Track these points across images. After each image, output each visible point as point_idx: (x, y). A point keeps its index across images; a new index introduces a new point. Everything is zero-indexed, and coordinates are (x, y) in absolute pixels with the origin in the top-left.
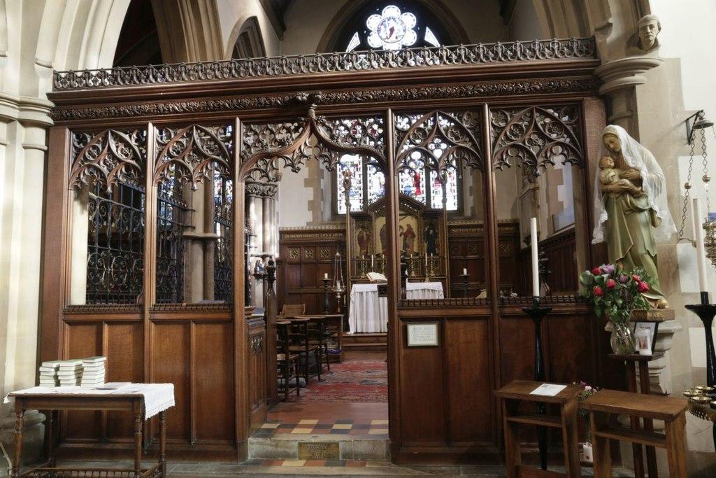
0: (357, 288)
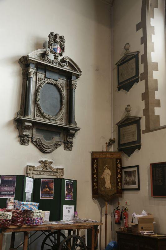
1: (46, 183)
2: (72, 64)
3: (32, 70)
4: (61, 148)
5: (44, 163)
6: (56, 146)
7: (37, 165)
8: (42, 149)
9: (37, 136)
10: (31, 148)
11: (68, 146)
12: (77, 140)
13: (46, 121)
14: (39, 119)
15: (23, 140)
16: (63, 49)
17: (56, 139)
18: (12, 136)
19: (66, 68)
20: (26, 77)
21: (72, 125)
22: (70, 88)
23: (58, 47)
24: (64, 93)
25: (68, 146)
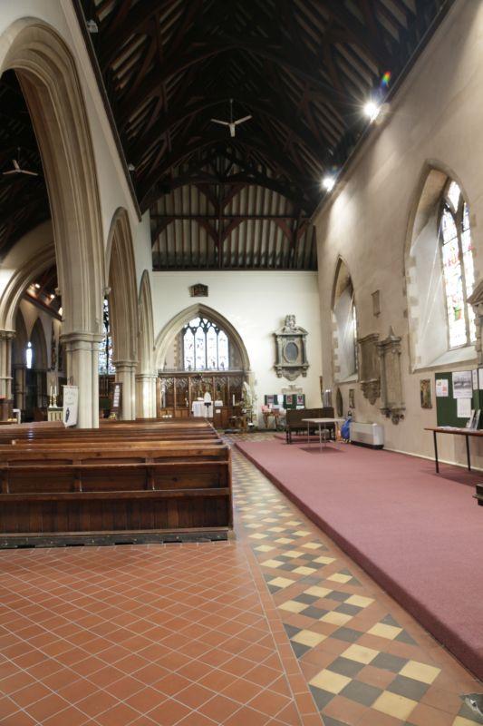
0: (194, 403)
1: (289, 397)
2: (301, 329)
3: (279, 340)
4: (300, 377)
5: (291, 386)
6: (297, 376)
7: (287, 387)
8: (287, 377)
9: (286, 373)
10: (283, 380)
11: (304, 375)
12: (309, 372)
13: (290, 365)
14: (286, 365)
15: (279, 376)
16: (294, 322)
17: (296, 373)
18: (274, 373)
19: (299, 332)
20: (276, 343)
21: (305, 364)
22: (303, 344)
23: (292, 322)
24: (299, 346)
25: (304, 375)
